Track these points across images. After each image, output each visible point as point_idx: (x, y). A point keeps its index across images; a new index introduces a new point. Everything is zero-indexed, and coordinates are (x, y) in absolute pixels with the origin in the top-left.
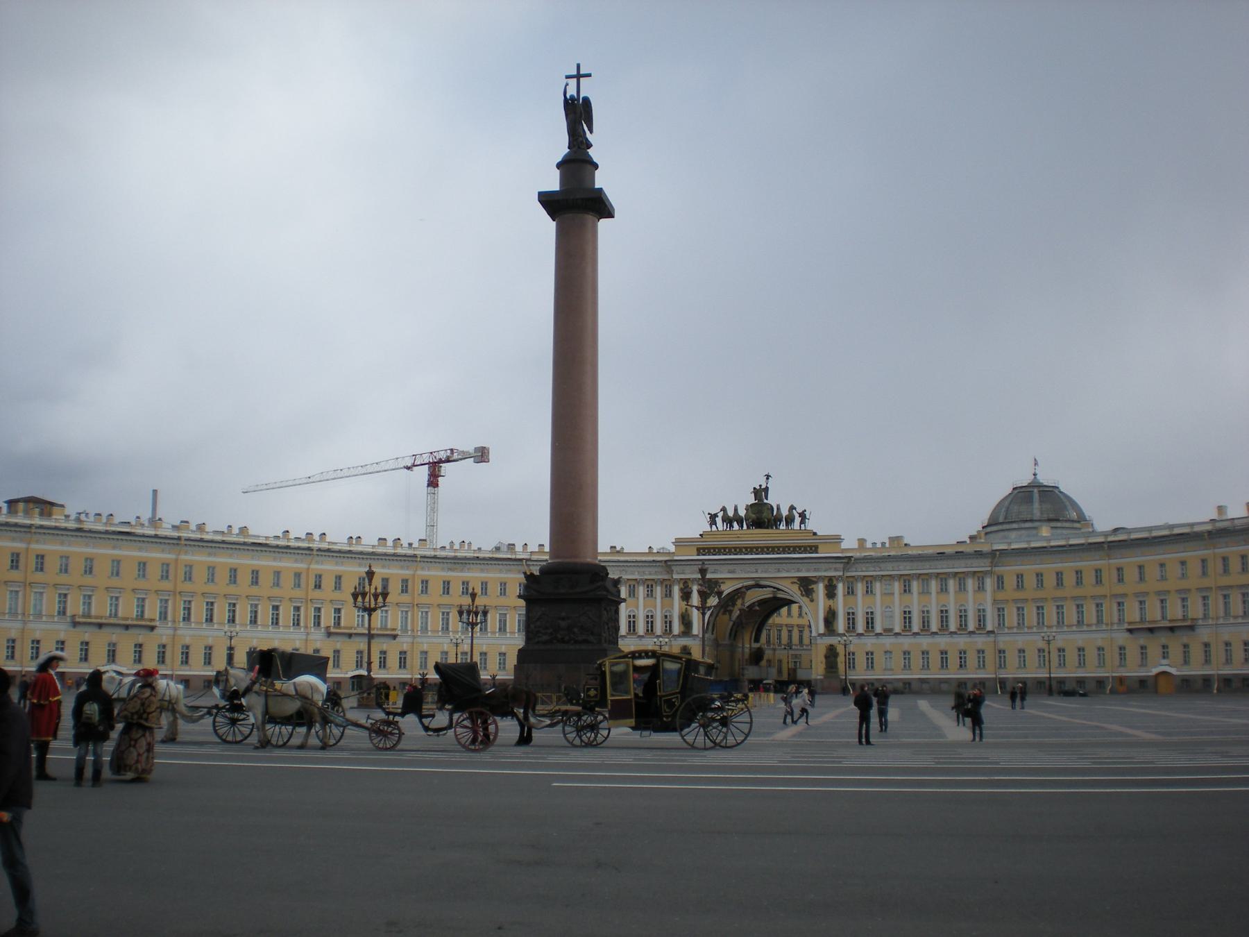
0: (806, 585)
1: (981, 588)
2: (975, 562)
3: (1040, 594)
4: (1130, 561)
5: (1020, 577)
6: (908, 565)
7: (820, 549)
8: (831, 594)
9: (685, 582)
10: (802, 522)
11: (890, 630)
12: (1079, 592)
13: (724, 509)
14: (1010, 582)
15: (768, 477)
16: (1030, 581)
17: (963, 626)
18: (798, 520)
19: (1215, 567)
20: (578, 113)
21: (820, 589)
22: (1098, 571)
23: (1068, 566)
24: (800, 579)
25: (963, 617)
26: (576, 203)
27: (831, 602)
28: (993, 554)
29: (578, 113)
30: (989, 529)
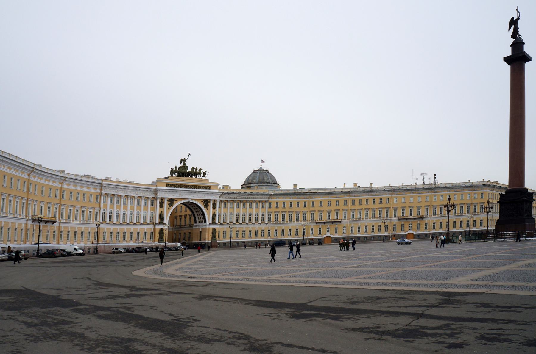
3: (291, 210)
4: (317, 199)
5: (277, 203)
8: (214, 208)
12: (298, 209)
14: (274, 205)
16: (280, 205)
17: (256, 221)
19: (350, 203)
21: (211, 205)
22: (305, 202)
23: (294, 200)
25: (257, 218)
27: (214, 210)
28: (271, 195)
30: (245, 186)
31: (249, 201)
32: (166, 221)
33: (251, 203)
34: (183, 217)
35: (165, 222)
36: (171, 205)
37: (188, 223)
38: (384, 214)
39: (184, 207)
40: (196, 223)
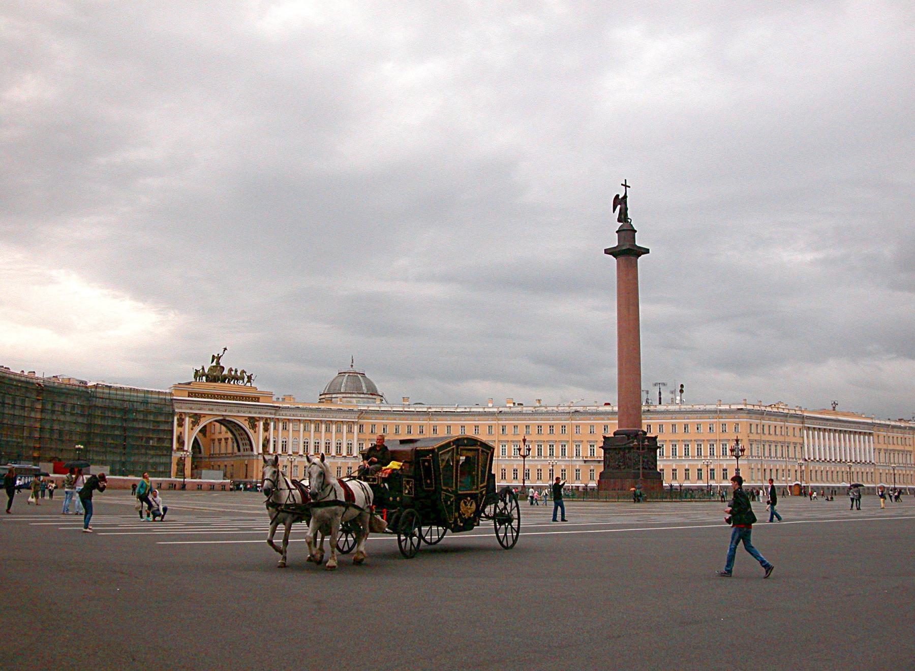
0: (253, 422)
1: (350, 431)
2: (349, 415)
6: (310, 414)
7: (261, 399)
8: (266, 429)
9: (181, 414)
10: (249, 381)
11: (297, 453)
13: (203, 369)
15: (225, 349)
17: (339, 452)
18: (246, 380)
20: (620, 202)
24: (250, 418)
26: (627, 251)
27: (266, 434)
29: (620, 202)
31: (326, 422)
32: (188, 446)
33: (329, 423)
34: (223, 441)
35: (186, 448)
36: (194, 424)
37: (230, 451)
38: (557, 450)
39: (218, 424)
40: (239, 450)
